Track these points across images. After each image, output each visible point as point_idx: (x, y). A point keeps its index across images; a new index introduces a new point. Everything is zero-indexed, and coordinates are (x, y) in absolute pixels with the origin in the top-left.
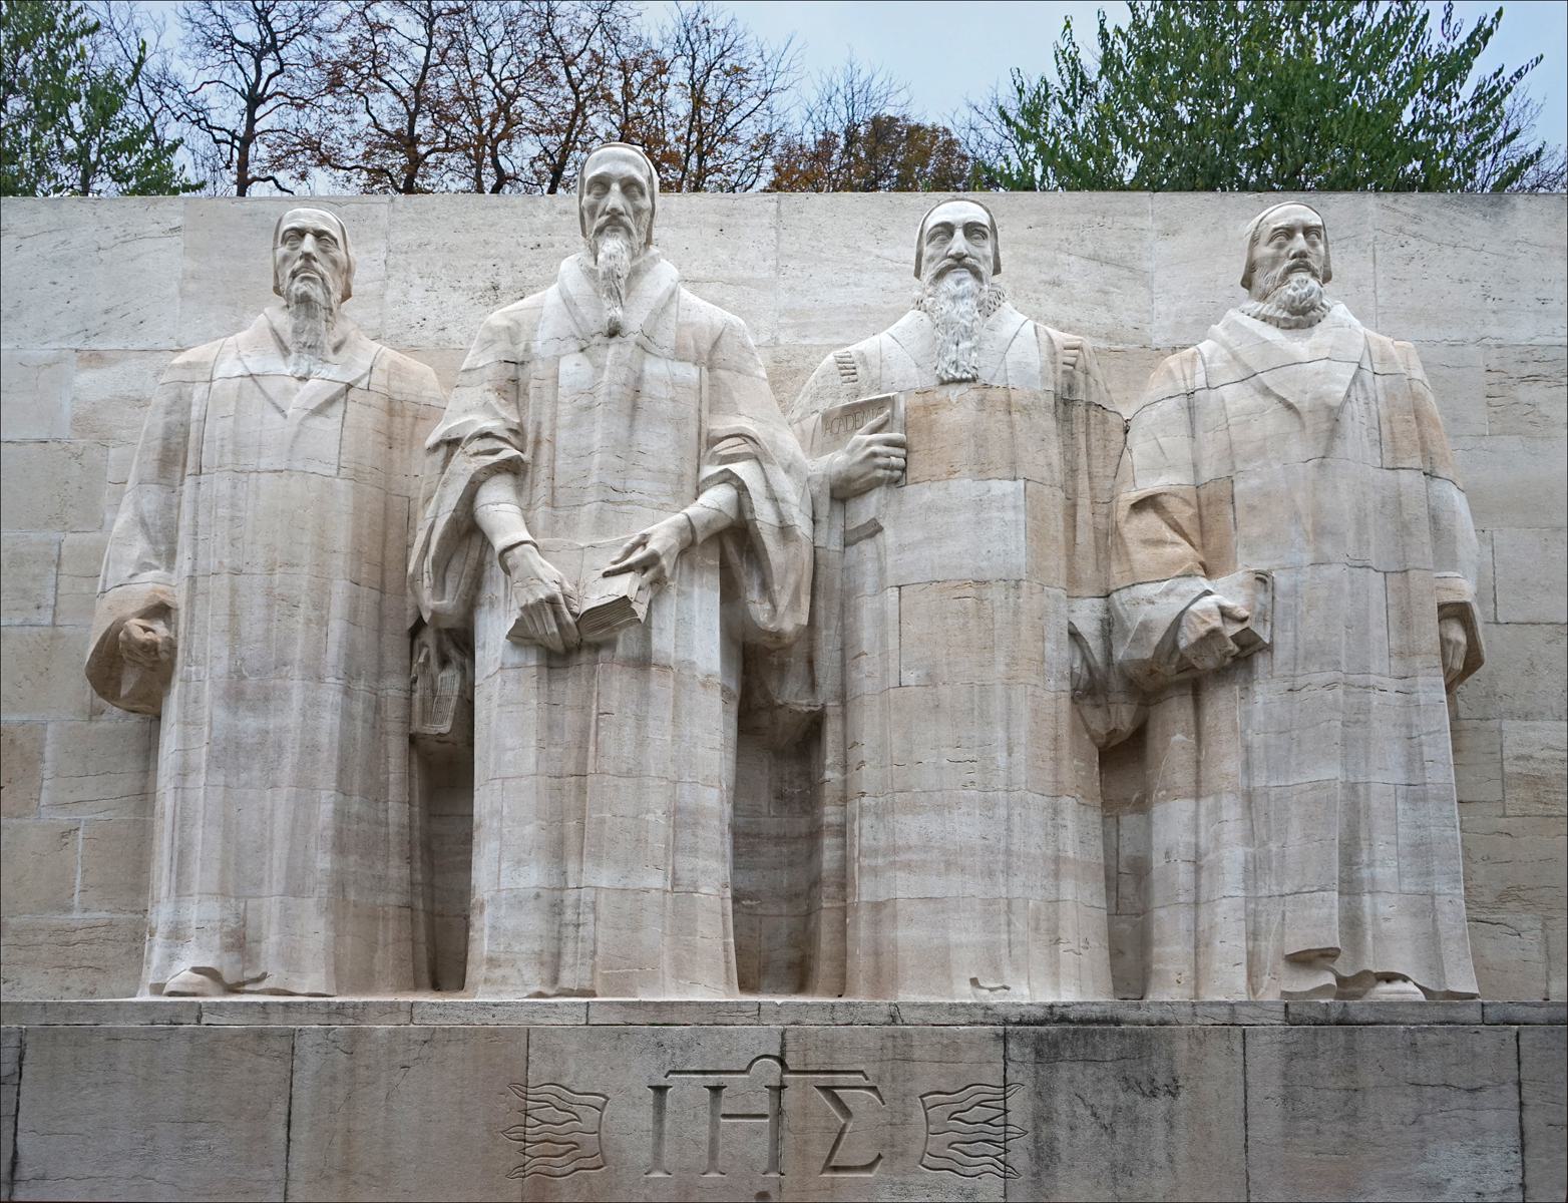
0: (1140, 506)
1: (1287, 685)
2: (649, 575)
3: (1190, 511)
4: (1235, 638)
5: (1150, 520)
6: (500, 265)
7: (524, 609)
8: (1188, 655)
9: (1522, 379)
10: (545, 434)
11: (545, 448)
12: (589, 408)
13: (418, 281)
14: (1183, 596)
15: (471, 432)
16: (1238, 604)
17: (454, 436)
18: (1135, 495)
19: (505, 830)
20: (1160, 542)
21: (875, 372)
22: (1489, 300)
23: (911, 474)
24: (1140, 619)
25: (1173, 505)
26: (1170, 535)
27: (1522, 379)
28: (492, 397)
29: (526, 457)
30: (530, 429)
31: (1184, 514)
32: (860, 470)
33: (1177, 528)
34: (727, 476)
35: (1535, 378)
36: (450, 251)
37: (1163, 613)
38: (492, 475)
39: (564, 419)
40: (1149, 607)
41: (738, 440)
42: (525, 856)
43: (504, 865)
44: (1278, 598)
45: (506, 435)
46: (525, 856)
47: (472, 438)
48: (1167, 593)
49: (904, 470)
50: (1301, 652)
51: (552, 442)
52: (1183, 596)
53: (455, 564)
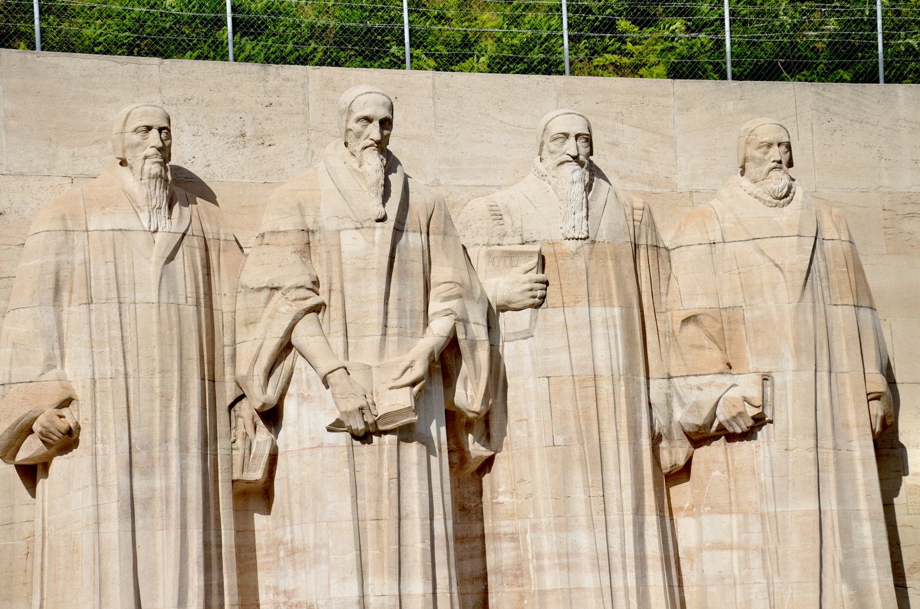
0: (686, 321)
1: (784, 447)
2: (416, 389)
3: (719, 326)
4: (754, 418)
5: (691, 328)
6: (245, 118)
7: (343, 413)
8: (726, 425)
9: (905, 216)
10: (336, 286)
11: (336, 297)
12: (365, 269)
13: (187, 128)
14: (719, 387)
15: (288, 284)
16: (754, 394)
17: (276, 285)
18: (684, 314)
19: (332, 557)
20: (701, 347)
21: (518, 224)
22: (883, 160)
23: (548, 300)
24: (694, 399)
25: (707, 321)
26: (707, 343)
27: (905, 216)
28: (295, 258)
29: (323, 298)
30: (323, 281)
31: (714, 330)
32: (518, 297)
33: (711, 338)
34: (449, 312)
35: (911, 215)
36: (208, 106)
37: (708, 398)
38: (305, 314)
39: (349, 272)
40: (698, 392)
41: (451, 285)
42: (348, 575)
43: (332, 581)
44: (776, 390)
45: (311, 286)
46: (348, 575)
47: (290, 288)
48: (710, 384)
49: (543, 298)
50: (791, 426)
51: (342, 292)
52: (719, 387)
53: (278, 370)
